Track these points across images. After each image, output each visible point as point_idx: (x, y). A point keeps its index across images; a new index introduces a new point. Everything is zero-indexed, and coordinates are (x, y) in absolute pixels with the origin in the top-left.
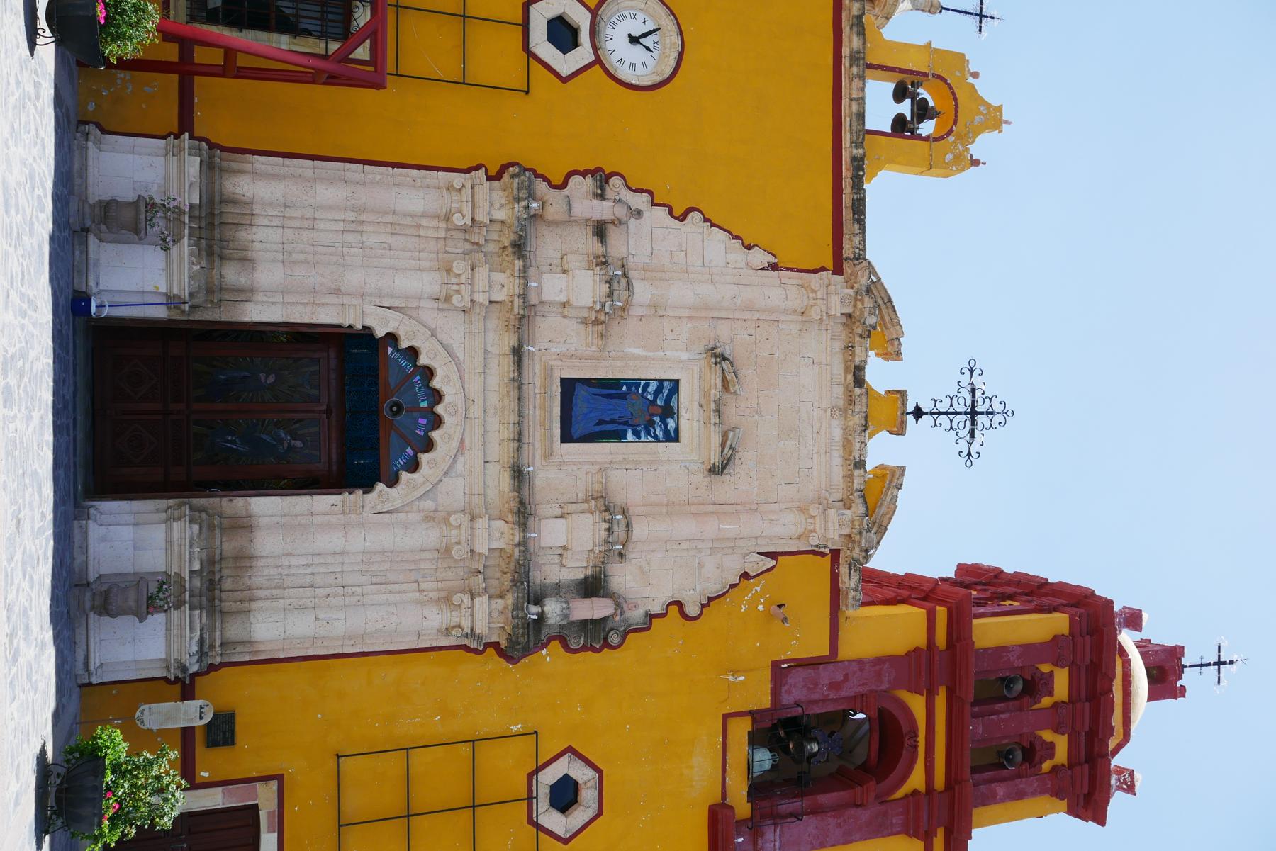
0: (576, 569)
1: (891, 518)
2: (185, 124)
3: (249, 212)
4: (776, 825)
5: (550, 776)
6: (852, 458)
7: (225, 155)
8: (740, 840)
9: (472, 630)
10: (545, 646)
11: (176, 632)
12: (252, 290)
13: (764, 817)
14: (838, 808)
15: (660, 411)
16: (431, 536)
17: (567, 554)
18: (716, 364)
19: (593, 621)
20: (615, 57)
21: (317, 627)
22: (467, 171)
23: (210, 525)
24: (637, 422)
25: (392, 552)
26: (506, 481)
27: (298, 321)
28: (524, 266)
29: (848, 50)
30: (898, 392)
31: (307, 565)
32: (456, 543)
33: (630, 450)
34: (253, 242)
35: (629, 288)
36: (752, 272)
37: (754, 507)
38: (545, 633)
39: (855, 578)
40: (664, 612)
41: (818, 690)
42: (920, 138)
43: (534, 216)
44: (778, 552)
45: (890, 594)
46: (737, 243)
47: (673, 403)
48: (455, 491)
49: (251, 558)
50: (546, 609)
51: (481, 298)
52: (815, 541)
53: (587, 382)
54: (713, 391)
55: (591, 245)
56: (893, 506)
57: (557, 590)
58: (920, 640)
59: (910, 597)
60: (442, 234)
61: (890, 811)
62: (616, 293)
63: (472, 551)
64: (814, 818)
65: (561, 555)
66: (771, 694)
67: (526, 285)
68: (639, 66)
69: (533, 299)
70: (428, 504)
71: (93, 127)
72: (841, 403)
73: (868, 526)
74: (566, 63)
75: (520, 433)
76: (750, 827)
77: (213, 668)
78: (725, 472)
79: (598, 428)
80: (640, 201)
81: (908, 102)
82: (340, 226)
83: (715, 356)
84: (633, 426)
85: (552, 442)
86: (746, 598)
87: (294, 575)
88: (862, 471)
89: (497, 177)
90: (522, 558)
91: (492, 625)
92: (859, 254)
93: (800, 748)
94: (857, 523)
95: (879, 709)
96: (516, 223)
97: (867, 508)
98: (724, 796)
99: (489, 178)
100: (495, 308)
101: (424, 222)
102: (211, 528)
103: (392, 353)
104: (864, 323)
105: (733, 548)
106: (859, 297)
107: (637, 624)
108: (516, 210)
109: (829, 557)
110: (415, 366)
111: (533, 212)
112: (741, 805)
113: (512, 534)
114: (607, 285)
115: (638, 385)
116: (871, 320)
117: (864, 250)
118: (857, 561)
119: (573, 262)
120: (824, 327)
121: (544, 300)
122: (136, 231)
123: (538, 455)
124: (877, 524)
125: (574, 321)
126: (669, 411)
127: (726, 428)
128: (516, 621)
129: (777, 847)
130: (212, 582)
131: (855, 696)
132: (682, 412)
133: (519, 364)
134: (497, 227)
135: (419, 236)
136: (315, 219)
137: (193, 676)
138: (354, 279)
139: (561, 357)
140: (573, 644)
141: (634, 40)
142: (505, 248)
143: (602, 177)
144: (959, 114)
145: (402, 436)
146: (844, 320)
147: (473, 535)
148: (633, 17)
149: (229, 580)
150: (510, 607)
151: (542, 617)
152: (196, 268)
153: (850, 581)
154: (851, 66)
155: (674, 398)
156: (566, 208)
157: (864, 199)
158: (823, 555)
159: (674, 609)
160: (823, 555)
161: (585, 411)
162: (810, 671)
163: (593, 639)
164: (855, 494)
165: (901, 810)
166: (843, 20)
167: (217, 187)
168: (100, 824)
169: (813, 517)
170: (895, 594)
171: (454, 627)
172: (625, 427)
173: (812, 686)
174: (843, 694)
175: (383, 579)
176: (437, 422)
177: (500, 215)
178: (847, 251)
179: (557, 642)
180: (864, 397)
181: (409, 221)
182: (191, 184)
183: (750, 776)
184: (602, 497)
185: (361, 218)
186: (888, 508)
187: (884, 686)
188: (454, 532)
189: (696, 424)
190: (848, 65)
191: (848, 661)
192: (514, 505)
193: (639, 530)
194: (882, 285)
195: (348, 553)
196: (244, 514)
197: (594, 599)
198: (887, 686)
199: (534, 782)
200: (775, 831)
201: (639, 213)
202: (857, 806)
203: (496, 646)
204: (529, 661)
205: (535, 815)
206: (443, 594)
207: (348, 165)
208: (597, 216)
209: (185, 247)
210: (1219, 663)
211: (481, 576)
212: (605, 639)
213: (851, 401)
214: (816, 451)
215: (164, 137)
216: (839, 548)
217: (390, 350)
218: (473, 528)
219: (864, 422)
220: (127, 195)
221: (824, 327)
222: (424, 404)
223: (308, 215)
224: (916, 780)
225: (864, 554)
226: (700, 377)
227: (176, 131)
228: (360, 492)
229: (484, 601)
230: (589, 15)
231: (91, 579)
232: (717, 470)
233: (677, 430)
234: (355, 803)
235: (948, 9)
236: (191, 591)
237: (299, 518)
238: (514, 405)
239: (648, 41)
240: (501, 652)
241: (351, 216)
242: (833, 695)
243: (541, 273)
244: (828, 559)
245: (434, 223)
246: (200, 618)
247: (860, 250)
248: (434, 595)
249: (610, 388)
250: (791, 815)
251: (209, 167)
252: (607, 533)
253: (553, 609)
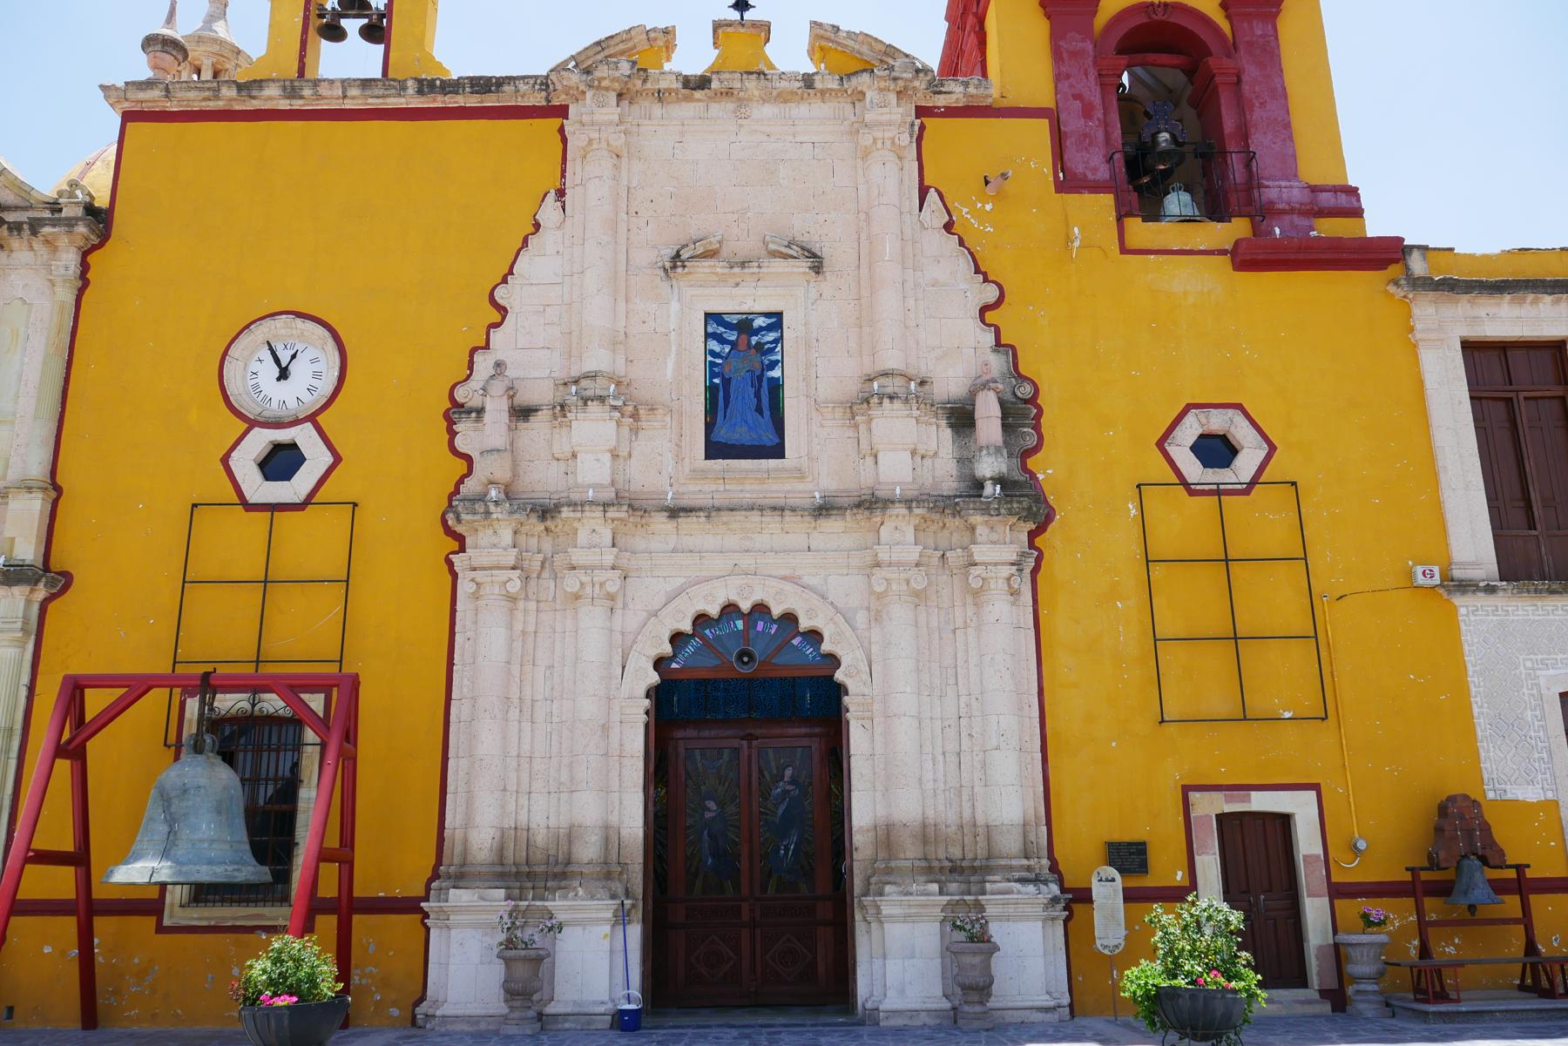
0: (941, 438)
1: (876, 40)
2: (410, 906)
3: (513, 832)
4: (1260, 186)
5: (1192, 469)
6: (800, 91)
7: (445, 860)
8: (1277, 231)
9: (1013, 564)
10: (1033, 475)
11: (1011, 909)
12: (606, 827)
13: (1250, 201)
14: (1242, 106)
15: (744, 337)
16: (899, 614)
17: (921, 450)
18: (684, 267)
19: (1004, 417)
20: (306, 397)
21: (1007, 747)
22: (454, 576)
23: (885, 872)
24: (758, 366)
25: (918, 661)
26: (832, 525)
27: (641, 774)
28: (569, 506)
29: (282, 102)
30: (715, 31)
31: (934, 760)
32: (908, 584)
33: (793, 374)
34: (548, 828)
35: (592, 376)
36: (568, 222)
37: (862, 216)
38: (1018, 476)
39: (951, 86)
40: (993, 328)
41: (1092, 132)
43: (507, 494)
44: (919, 185)
45: (972, 40)
46: (532, 240)
47: (734, 319)
48: (845, 587)
49: (924, 826)
50: (988, 475)
51: (609, 557)
52: (905, 139)
53: (709, 427)
54: (718, 270)
55: (540, 422)
56: (860, 38)
57: (965, 461)
59: (976, 14)
60: (532, 605)
61: (1248, 38)
62: (599, 392)
63: (917, 565)
64: (1253, 137)
65: (923, 457)
66: (1096, 193)
67: (592, 503)
68: (316, 367)
69: (609, 495)
70: (861, 619)
71: (418, 1010)
72: (730, 106)
73: (885, 70)
74: (316, 458)
75: (774, 509)
76: (1262, 218)
77: (1054, 867)
78: (819, 254)
79: (767, 413)
80: (484, 363)
81: (344, 23)
82: (526, 726)
83: (674, 267)
84: (763, 370)
85: (784, 470)
86: (976, 226)
87: (945, 776)
88: (816, 77)
89: (460, 539)
90: (926, 504)
91: (1008, 540)
92: (542, 84)
93: (1165, 155)
94: (882, 84)
95: (1117, 54)
96: (516, 516)
97: (865, 70)
98: (1223, 252)
99: (462, 549)
100: (620, 541)
101: (518, 627)
102: (889, 871)
103: (678, 663)
104: (629, 76)
105: (914, 242)
106: (596, 83)
107: (1008, 362)
108: (500, 516)
109: (925, 120)
110: (693, 636)
111: (502, 496)
112: (1236, 229)
113: (897, 516)
114: (589, 403)
115: (712, 364)
116: (625, 68)
117: (536, 77)
118: (930, 83)
119: (562, 446)
120: (635, 129)
121: (608, 480)
122: (539, 960)
123: (800, 486)
124: (884, 58)
125: (635, 444)
126: (744, 326)
127: (764, 252)
128: (1003, 511)
129: (1288, 184)
130: (953, 870)
131: (1101, 84)
132: (745, 308)
133: (689, 510)
134: (522, 539)
135: (535, 632)
136: (518, 756)
137: (1063, 890)
138: (589, 708)
139: (679, 459)
140: (1031, 441)
141: (284, 374)
142: (547, 529)
143: (455, 412)
145: (779, 649)
146: (625, 103)
147: (899, 564)
148: (255, 376)
149: (951, 850)
150: (986, 518)
151: (999, 480)
152: (581, 892)
153: (956, 92)
154: (302, 97)
156: (495, 456)
157: (471, 79)
158: (922, 128)
159: (990, 316)
160: (922, 128)
161: (745, 429)
162: (1068, 143)
163: (1026, 416)
164: (846, 86)
165: (1245, 25)
166: (245, 108)
167: (484, 869)
168: (1234, 991)
169: (875, 140)
170: (972, 34)
171: (1010, 586)
172: (765, 380)
173: (1087, 140)
174: (1097, 100)
175: (951, 672)
176: (761, 609)
177: (506, 536)
178: (538, 99)
179: (1028, 461)
180: (723, 76)
181: (518, 645)
182: (482, 898)
183: (1198, 219)
184: (851, 407)
185: (516, 701)
186: (863, 44)
187: (1089, 47)
188: (894, 587)
189: (760, 291)
190: (301, 102)
191: (1056, 94)
192: (862, 515)
193: (892, 361)
194: (579, 53)
195: (919, 713)
196: (872, 834)
197: (976, 416)
198: (1089, 42)
199: (1199, 487)
200: (1267, 187)
201: (499, 365)
202: (1239, 81)
203: (1032, 535)
204: (1053, 495)
205: (1239, 487)
206: (969, 600)
207: (453, 718)
208: (505, 417)
209: (559, 906)
211: (948, 554)
212: (1026, 401)
213: (728, 93)
214: (791, 138)
215: (428, 930)
216: (914, 108)
217: (674, 665)
218: (890, 564)
219: (755, 76)
220: (495, 973)
221: (635, 129)
222: (740, 624)
223: (515, 764)
225: (921, 75)
226: (701, 286)
227: (419, 917)
228: (846, 700)
229: (979, 550)
230: (256, 430)
231: (948, 1005)
232: (817, 263)
233: (767, 315)
234: (1219, 701)
236: (963, 893)
237: (877, 770)
238: (739, 516)
239: (285, 358)
240: (1040, 530)
241: (514, 714)
242: (1099, 114)
243: (577, 485)
244: (928, 121)
245: (519, 615)
246: (995, 883)
247: (536, 83)
248: (970, 610)
249: (717, 398)
250: (1248, 166)
251: (461, 878)
252: (895, 401)
253: (988, 466)
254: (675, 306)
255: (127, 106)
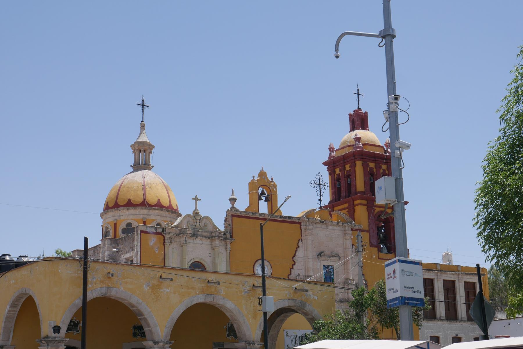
46: (298, 249)
58: (365, 208)
72: (325, 226)
126: (328, 267)
132: (329, 265)
144: (265, 185)
155: (326, 266)
178: (297, 221)
210: (358, 94)
213: (326, 224)
232: (340, 257)
233: (332, 266)
235: (143, 119)
254: (319, 263)
255: (233, 214)
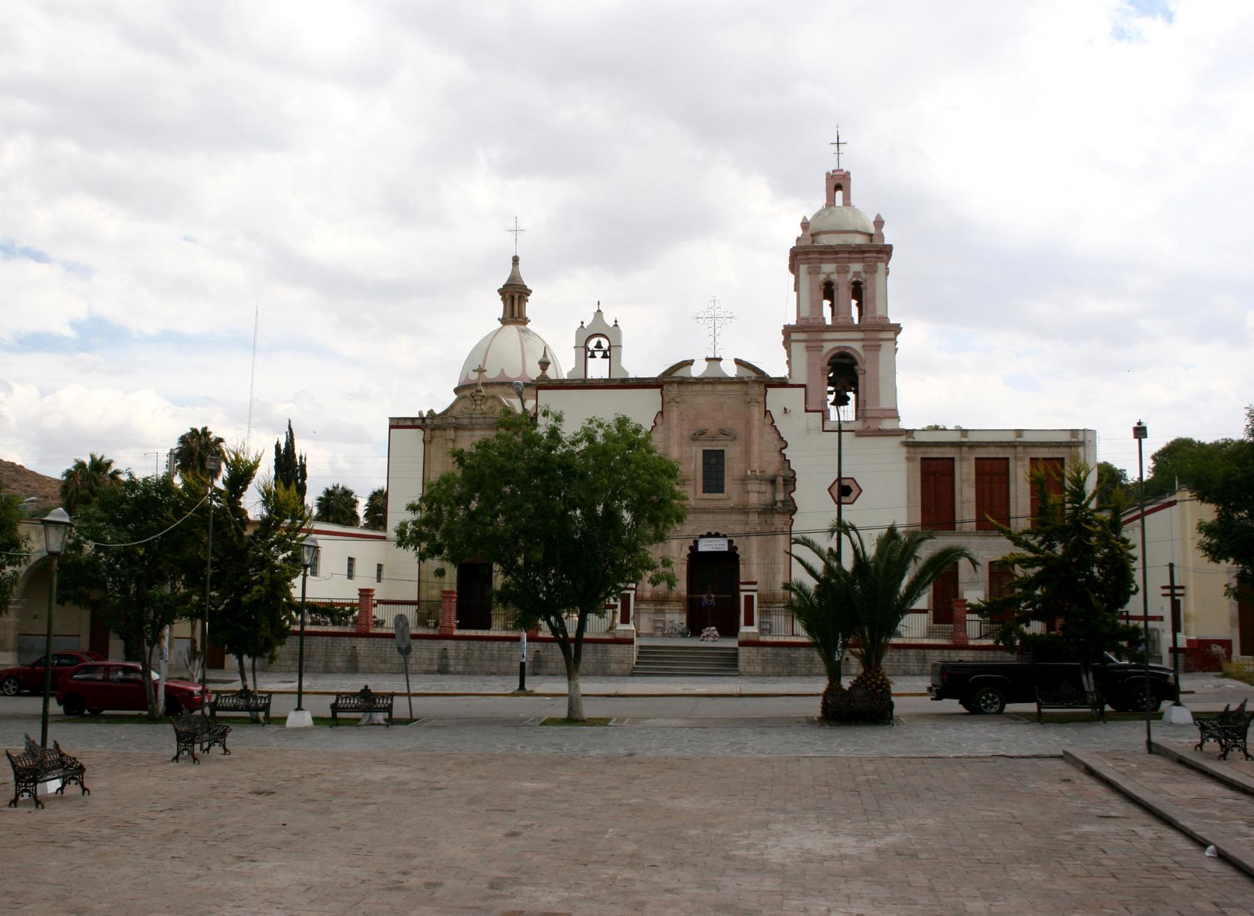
0: (766, 488)
42: (609, 349)
151: (782, 502)
224: (857, 346)
